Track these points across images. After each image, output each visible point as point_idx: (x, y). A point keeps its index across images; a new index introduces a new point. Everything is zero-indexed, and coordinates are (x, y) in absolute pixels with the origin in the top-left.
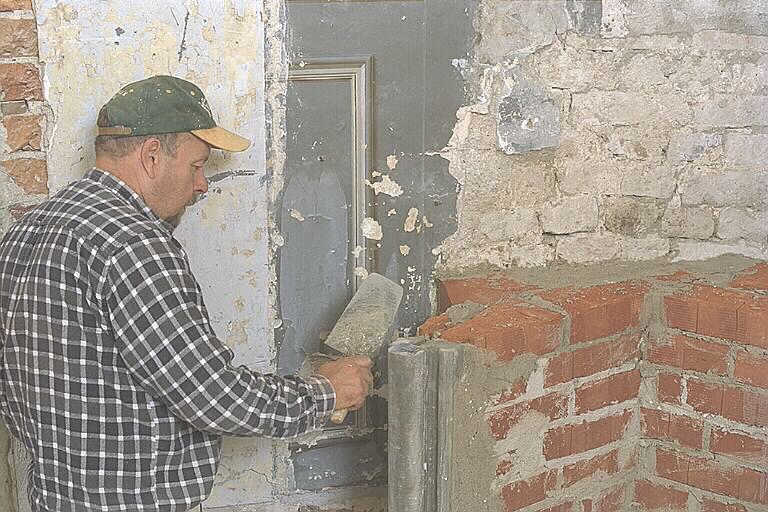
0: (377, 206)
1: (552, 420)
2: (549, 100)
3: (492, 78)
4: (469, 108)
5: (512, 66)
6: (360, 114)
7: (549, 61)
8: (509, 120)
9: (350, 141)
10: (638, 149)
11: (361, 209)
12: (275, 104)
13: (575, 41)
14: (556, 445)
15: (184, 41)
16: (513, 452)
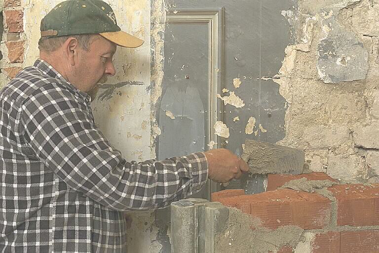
0: (225, 114)
3: (312, 25)
4: (294, 47)
5: (329, 16)
6: (214, 47)
7: (359, 14)
8: (326, 57)
9: (208, 65)
11: (214, 114)
12: (157, 38)
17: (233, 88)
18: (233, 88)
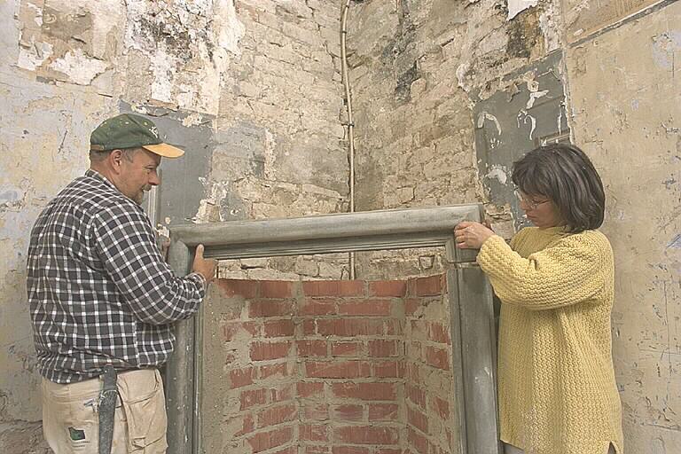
13: (254, 179)
14: (258, 352)
16: (234, 350)
17: (165, 224)
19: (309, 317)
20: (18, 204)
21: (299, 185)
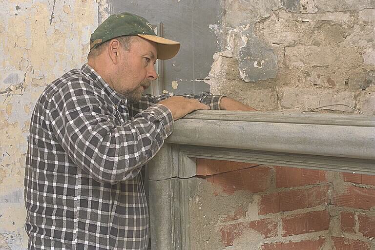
1: (266, 237)
2: (270, 49)
3: (233, 36)
4: (221, 53)
7: (269, 27)
10: (329, 81)
13: (284, 15)
15: (53, 13)
17: (172, 90)
18: (172, 90)
19: (348, 209)
20: (21, 86)
21: (353, 12)
